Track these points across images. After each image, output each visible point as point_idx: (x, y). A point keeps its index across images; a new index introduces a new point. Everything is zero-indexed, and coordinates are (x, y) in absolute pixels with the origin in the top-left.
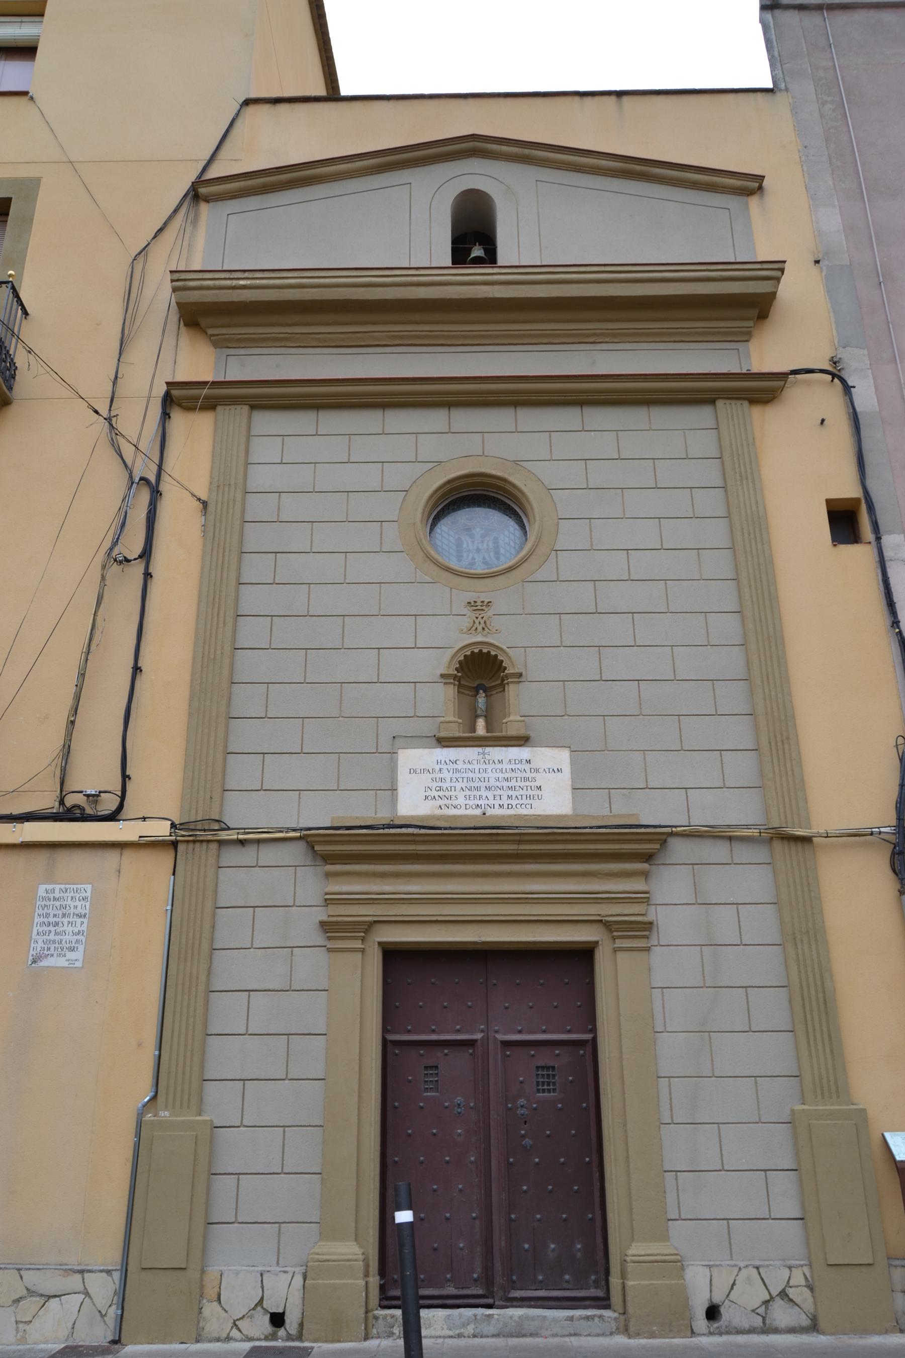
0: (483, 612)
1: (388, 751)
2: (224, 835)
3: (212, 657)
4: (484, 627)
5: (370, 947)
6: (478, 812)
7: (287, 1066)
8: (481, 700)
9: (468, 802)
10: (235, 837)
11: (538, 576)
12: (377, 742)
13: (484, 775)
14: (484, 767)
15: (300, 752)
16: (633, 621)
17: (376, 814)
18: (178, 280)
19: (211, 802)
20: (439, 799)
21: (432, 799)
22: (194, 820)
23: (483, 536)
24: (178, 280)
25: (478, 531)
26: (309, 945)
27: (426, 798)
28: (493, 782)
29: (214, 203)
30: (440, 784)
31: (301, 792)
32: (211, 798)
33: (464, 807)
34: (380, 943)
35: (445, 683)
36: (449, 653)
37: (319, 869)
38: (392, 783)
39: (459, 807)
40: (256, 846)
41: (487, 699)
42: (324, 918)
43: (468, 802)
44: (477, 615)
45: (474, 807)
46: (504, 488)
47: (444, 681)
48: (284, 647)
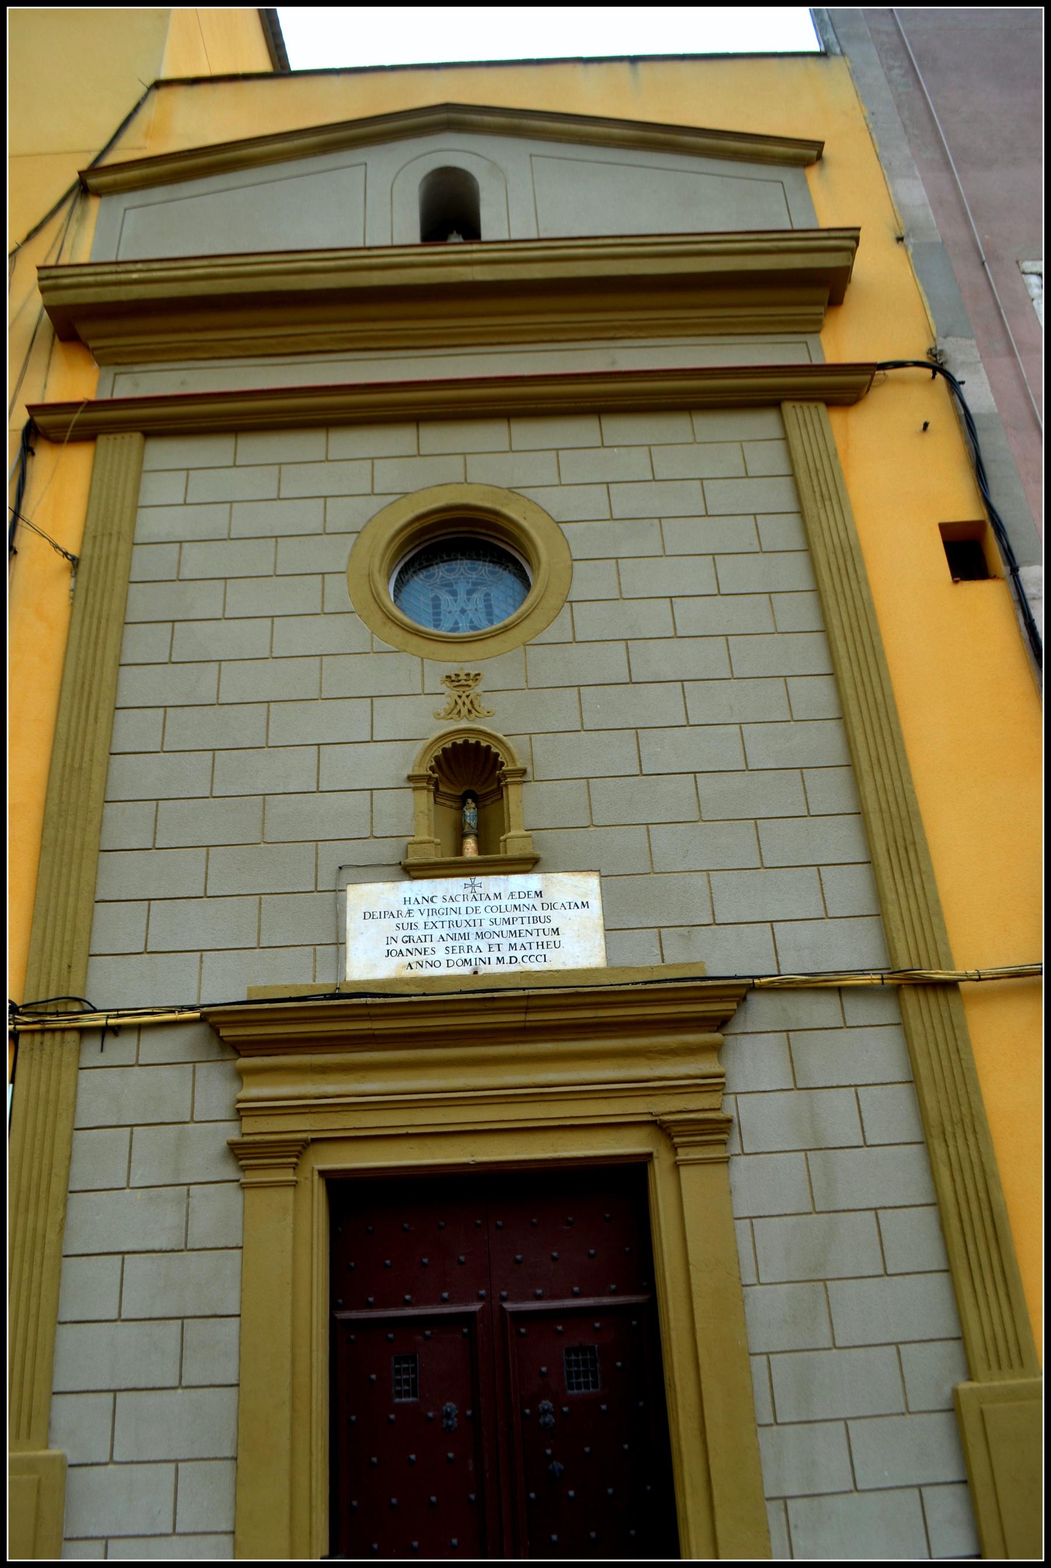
0: (468, 689)
1: (332, 889)
2: (87, 1021)
3: (76, 765)
4: (470, 708)
5: (306, 1179)
6: (467, 970)
7: (181, 1366)
8: (470, 812)
9: (450, 956)
10: (103, 1022)
11: (546, 636)
12: (316, 876)
13: (475, 916)
14: (474, 904)
15: (202, 895)
16: (684, 693)
17: (314, 981)
18: (48, 278)
19: (69, 972)
20: (409, 954)
21: (397, 955)
22: (44, 999)
23: (470, 593)
24: (48, 278)
25: (462, 589)
26: (214, 1180)
27: (389, 953)
28: (487, 926)
29: (108, 198)
30: (409, 932)
31: (204, 953)
32: (70, 967)
33: (444, 963)
34: (322, 1173)
35: (415, 789)
36: (420, 746)
37: (229, 1065)
38: (337, 933)
39: (437, 964)
40: (136, 1035)
41: (478, 811)
42: (235, 1137)
43: (450, 956)
44: (460, 693)
45: (460, 963)
46: (496, 524)
47: (412, 785)
48: (182, 749)
